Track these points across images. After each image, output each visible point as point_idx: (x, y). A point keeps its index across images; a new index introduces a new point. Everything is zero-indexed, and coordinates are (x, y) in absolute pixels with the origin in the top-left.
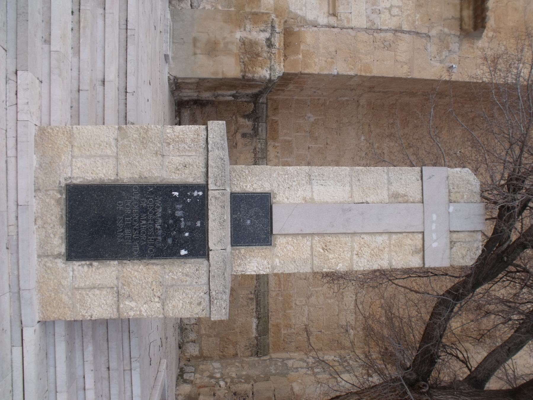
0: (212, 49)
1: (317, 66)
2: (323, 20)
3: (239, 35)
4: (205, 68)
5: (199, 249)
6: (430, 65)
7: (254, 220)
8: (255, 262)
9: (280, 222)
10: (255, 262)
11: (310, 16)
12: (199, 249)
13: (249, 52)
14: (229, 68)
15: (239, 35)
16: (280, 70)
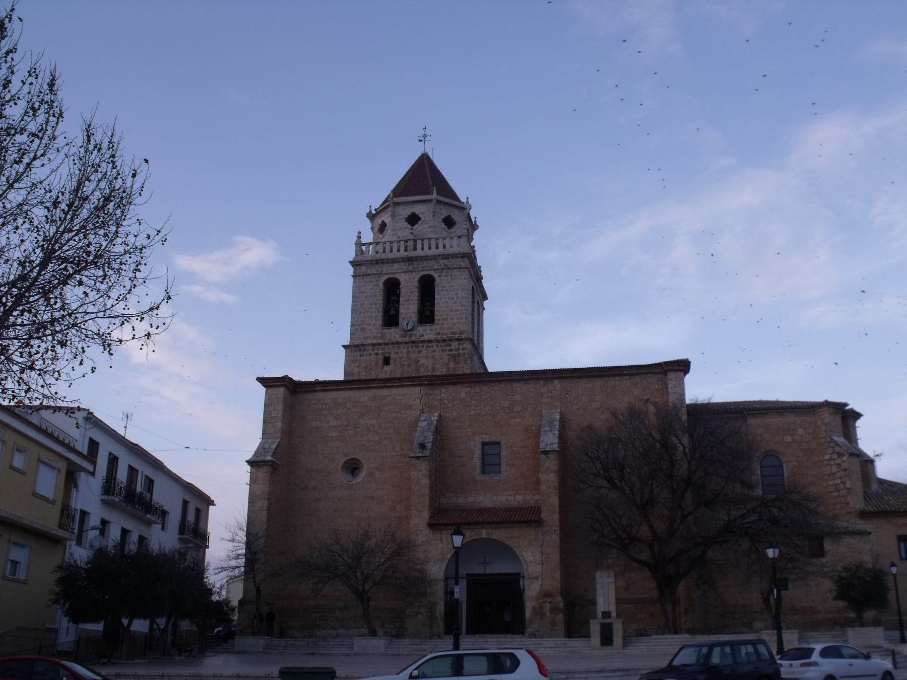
0: (554, 624)
1: (557, 584)
2: (540, 582)
3: (548, 614)
4: (561, 626)
5: (611, 624)
6: (554, 539)
7: (606, 614)
8: (614, 614)
9: (606, 610)
10: (614, 614)
11: (539, 587)
12: (611, 624)
13: (554, 610)
14: (560, 617)
15: (548, 614)
16: (559, 599)
